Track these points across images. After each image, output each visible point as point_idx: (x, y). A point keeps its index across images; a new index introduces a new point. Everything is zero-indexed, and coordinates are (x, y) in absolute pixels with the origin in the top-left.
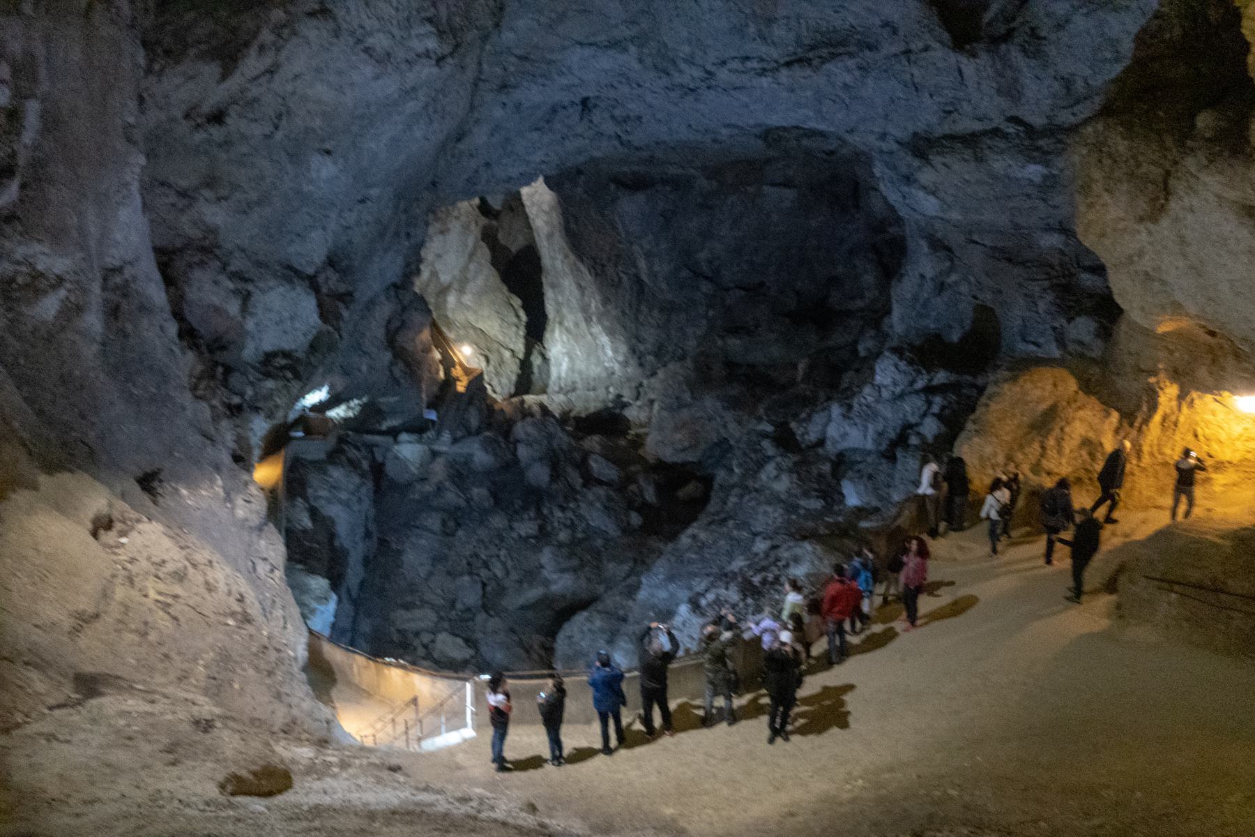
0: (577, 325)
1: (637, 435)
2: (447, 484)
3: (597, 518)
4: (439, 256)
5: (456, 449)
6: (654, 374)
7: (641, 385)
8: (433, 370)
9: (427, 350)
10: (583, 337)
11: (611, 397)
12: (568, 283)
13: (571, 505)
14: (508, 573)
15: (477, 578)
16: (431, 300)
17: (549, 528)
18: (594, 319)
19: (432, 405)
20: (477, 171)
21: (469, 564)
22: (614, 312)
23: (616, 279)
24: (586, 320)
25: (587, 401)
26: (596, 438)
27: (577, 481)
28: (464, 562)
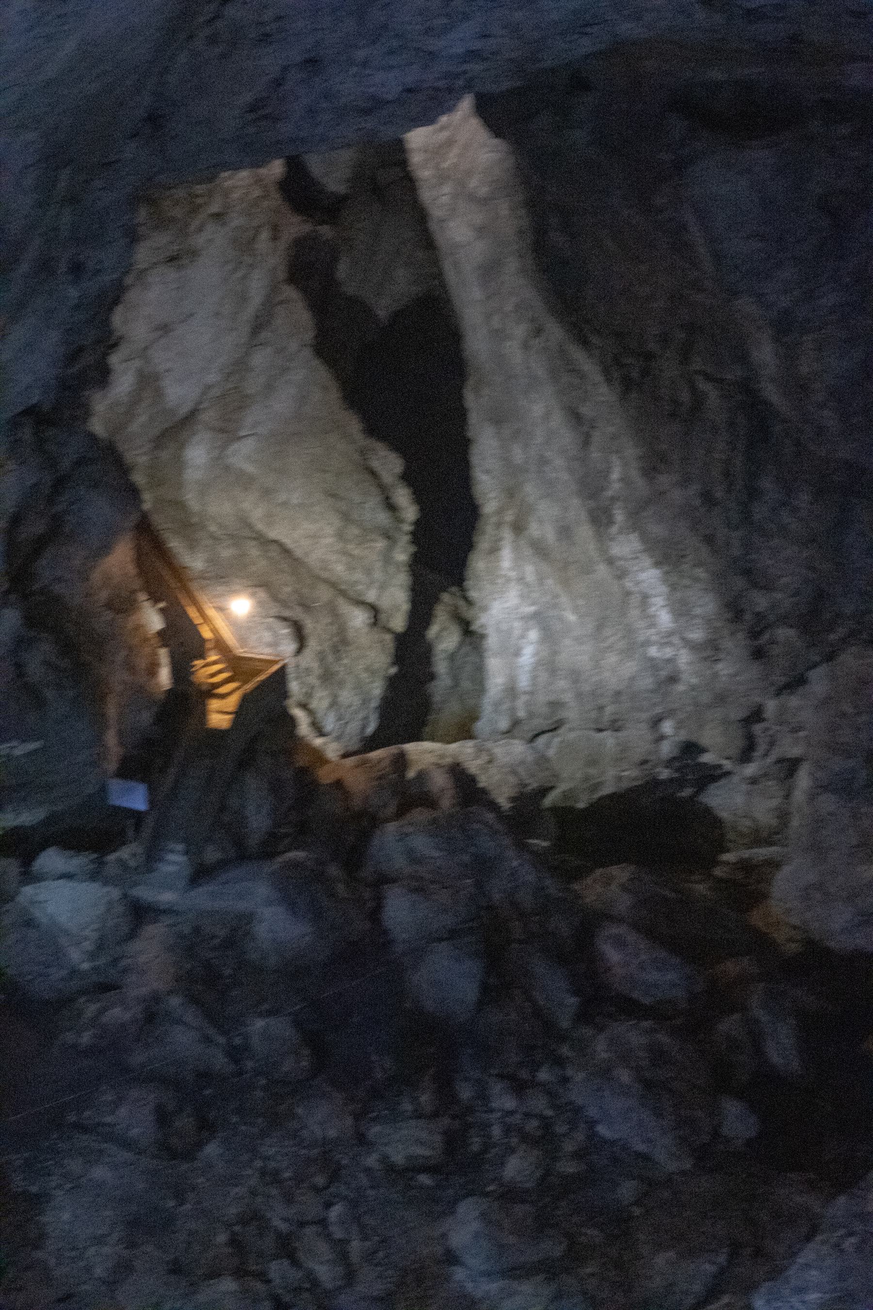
0: (565, 532)
1: (745, 866)
2: (175, 1001)
3: (621, 1119)
4: (164, 329)
5: (202, 898)
6: (796, 683)
7: (756, 715)
8: (142, 663)
9: (123, 605)
10: (587, 570)
11: (667, 749)
12: (542, 409)
13: (544, 1075)
14: (350, 1277)
15: (259, 1286)
16: (138, 455)
17: (476, 1144)
18: (619, 516)
19: (129, 770)
20: (278, 83)
21: (234, 1242)
22: (677, 495)
23: (685, 396)
25: (592, 762)
26: (621, 873)
27: (562, 1001)
28: (222, 1238)
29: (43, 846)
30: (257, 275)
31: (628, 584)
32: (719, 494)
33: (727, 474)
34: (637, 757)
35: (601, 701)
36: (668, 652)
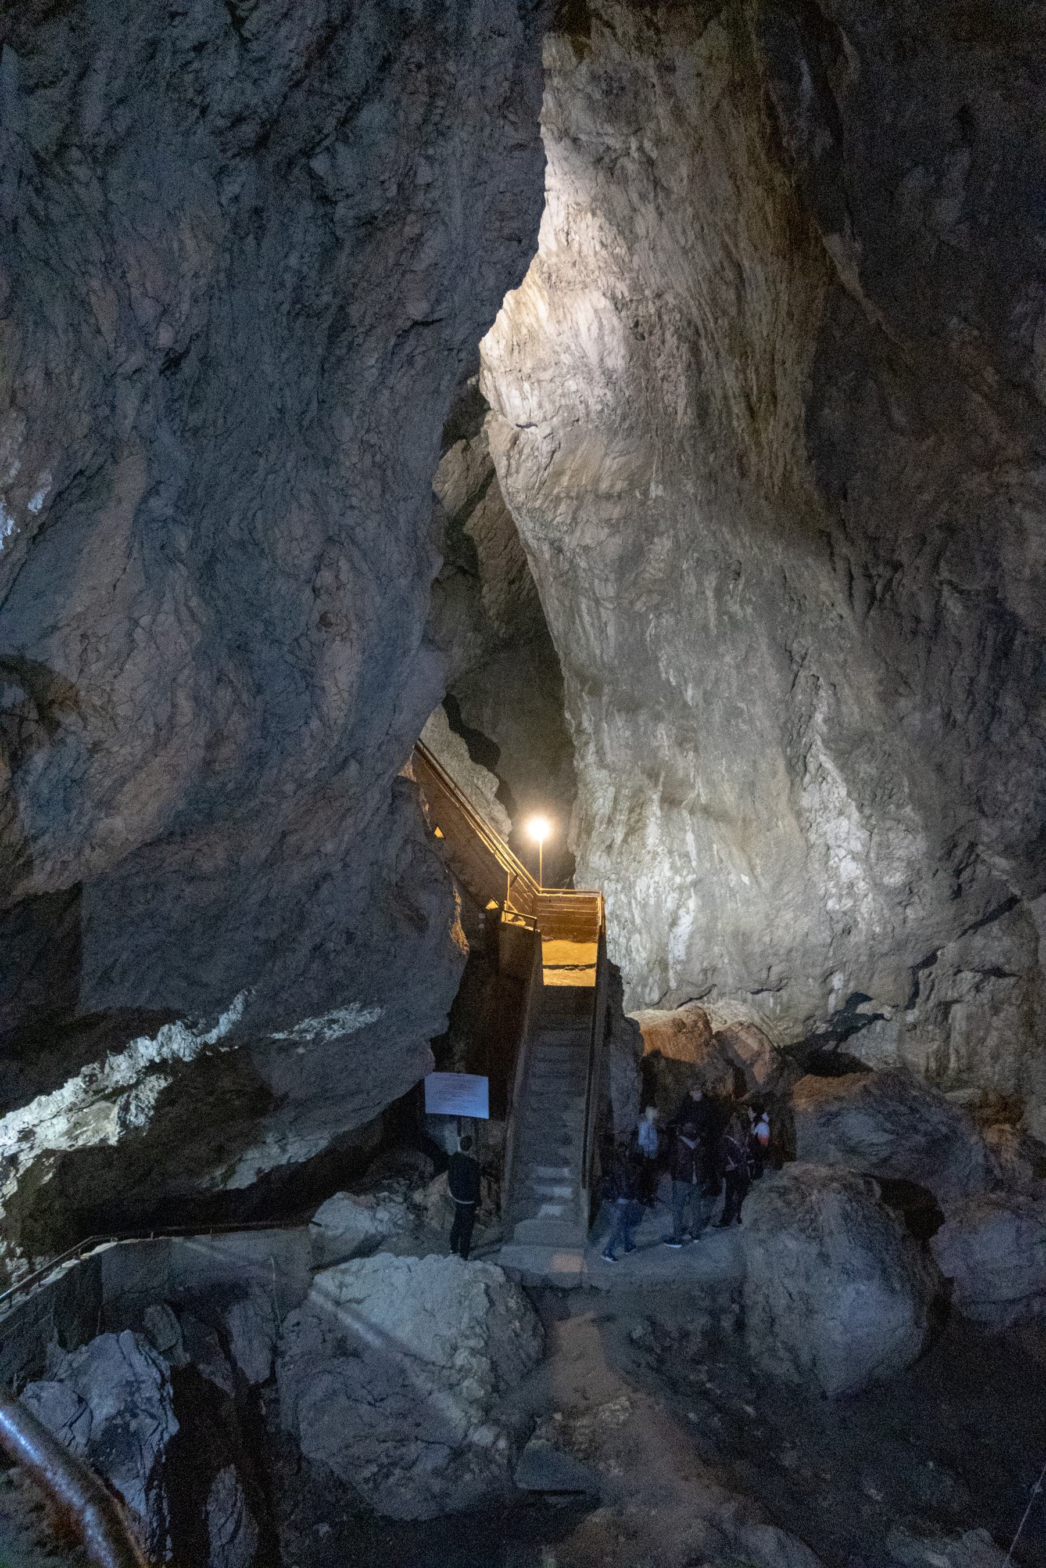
0: (749, 787)
23: (926, 611)
24: (791, 768)
29: (325, 1192)
31: (813, 837)
32: (959, 717)
33: (970, 693)
34: (802, 1016)
35: (771, 960)
36: (848, 903)
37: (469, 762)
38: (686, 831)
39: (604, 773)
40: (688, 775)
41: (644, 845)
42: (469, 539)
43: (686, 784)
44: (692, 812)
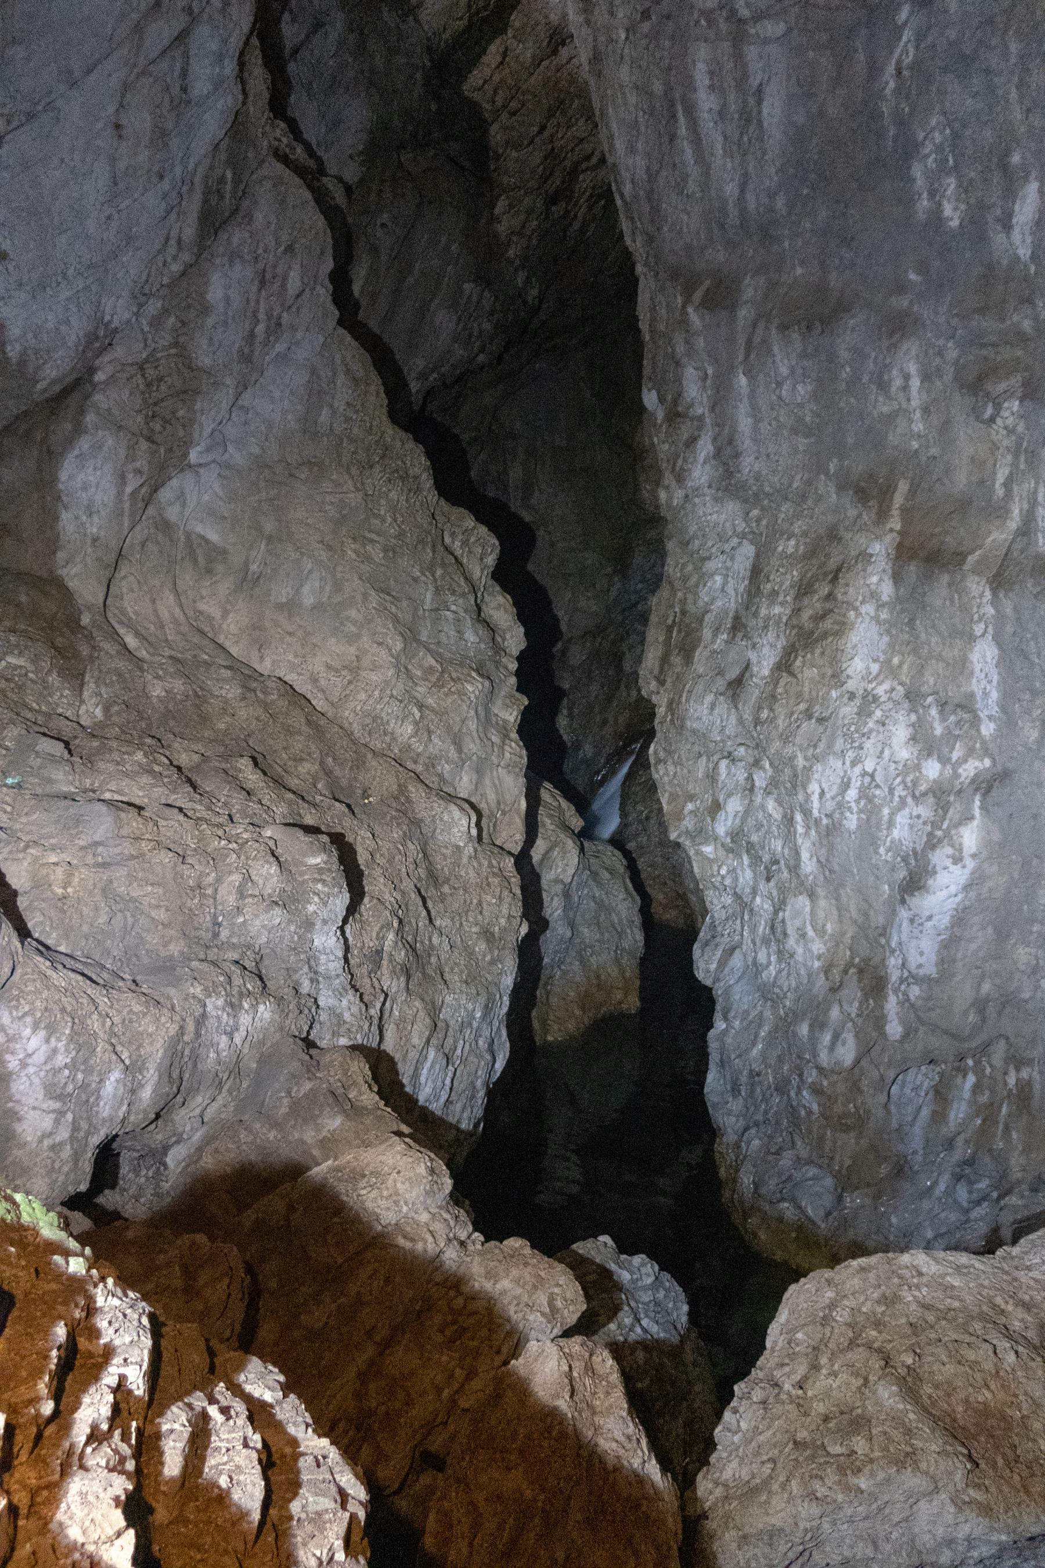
30: (206, 40)
37: (432, 496)
38: (971, 639)
39: (732, 507)
40: (984, 483)
41: (837, 678)
42: (474, 107)
43: (979, 505)
44: (999, 582)
